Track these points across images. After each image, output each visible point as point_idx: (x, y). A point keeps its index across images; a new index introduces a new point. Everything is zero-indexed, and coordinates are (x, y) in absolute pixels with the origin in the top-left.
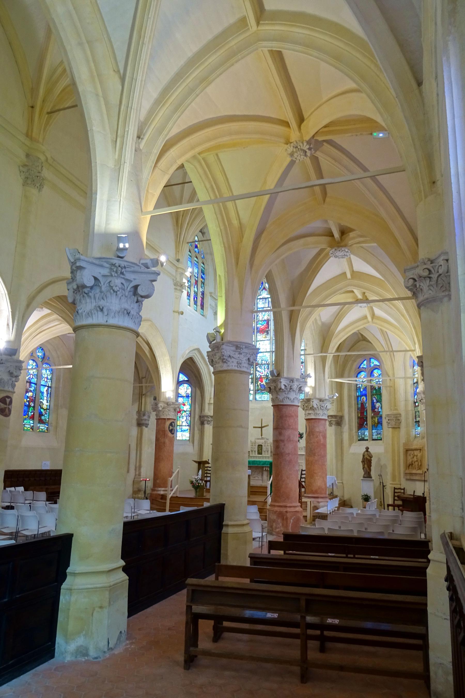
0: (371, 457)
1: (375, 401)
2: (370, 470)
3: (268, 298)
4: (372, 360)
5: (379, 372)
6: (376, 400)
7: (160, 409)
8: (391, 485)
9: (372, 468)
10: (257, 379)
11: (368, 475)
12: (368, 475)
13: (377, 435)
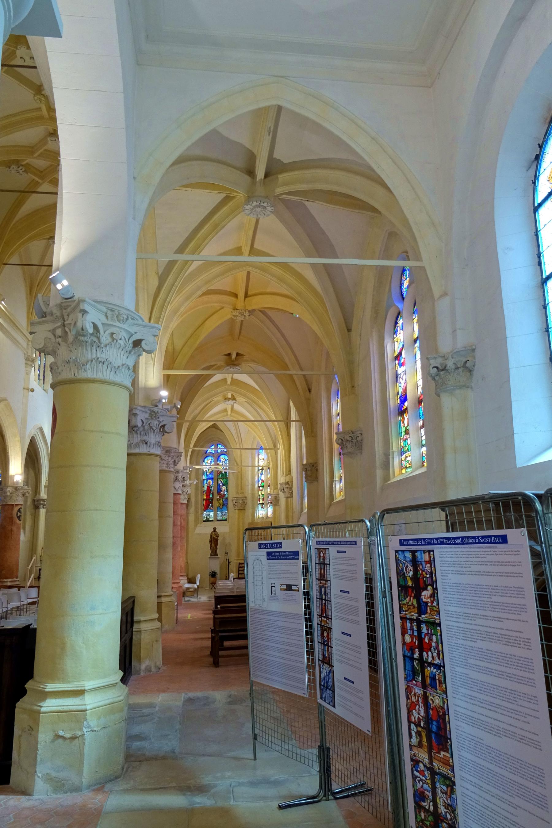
0: (218, 537)
1: (221, 484)
2: (217, 548)
4: (220, 446)
5: (226, 457)
7: (8, 494)
8: (235, 561)
9: (218, 547)
11: (214, 553)
12: (214, 553)
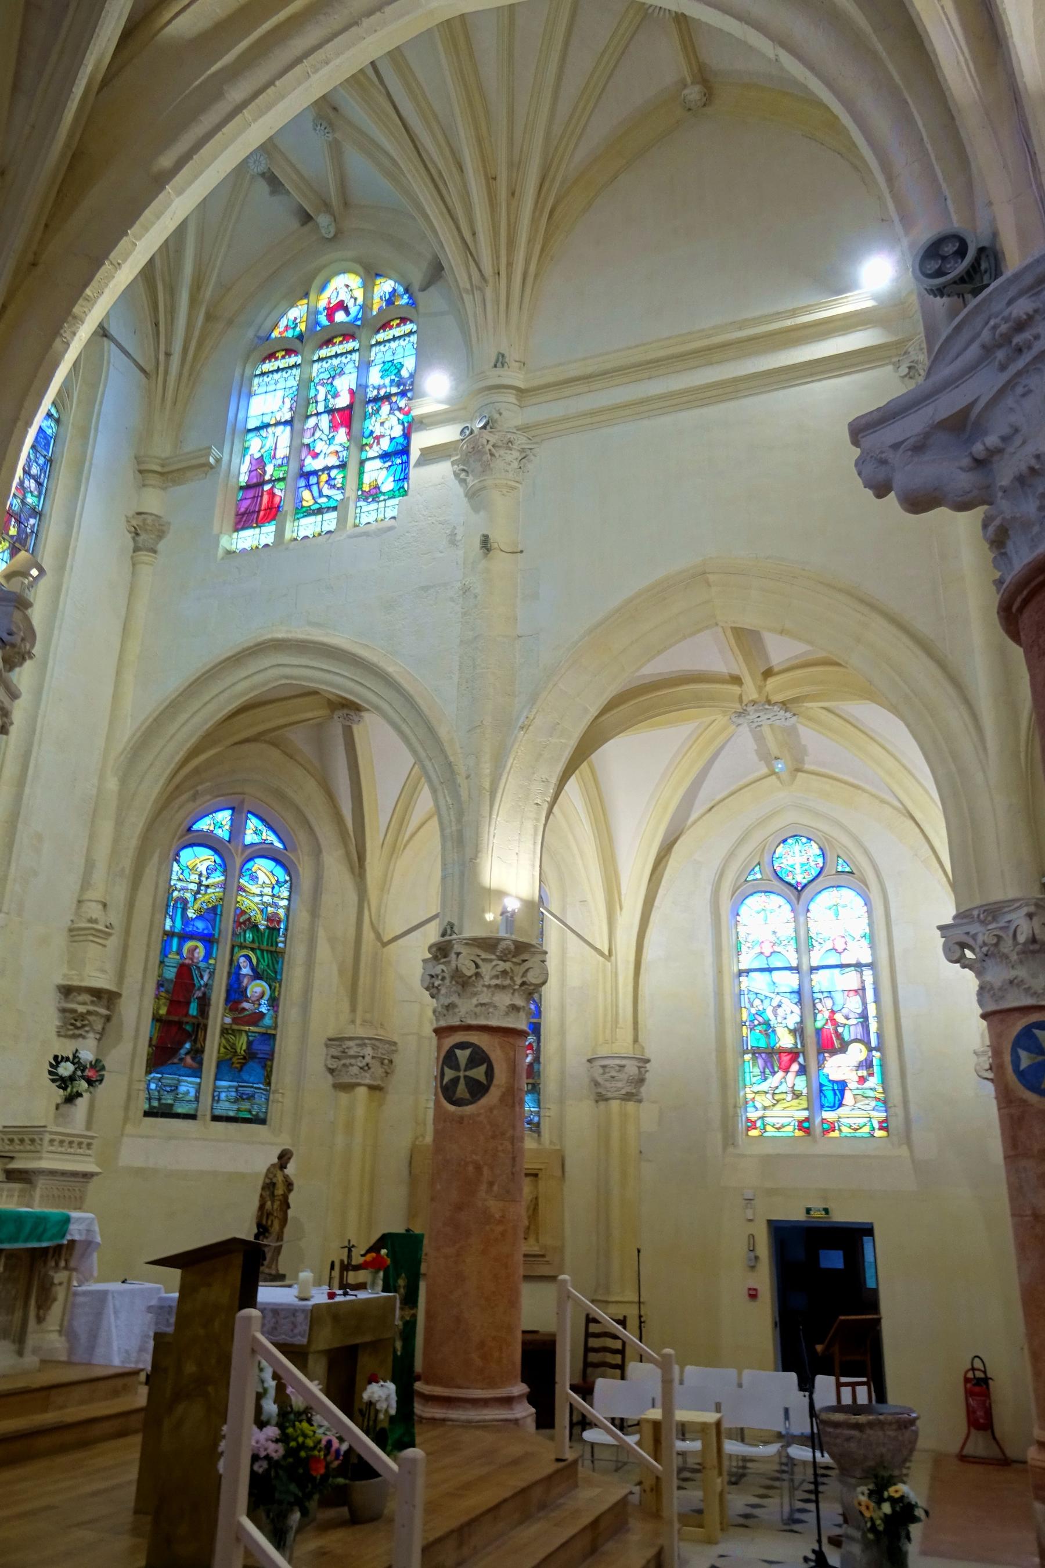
1: (246, 970)
6: (253, 969)
13: (236, 1101)
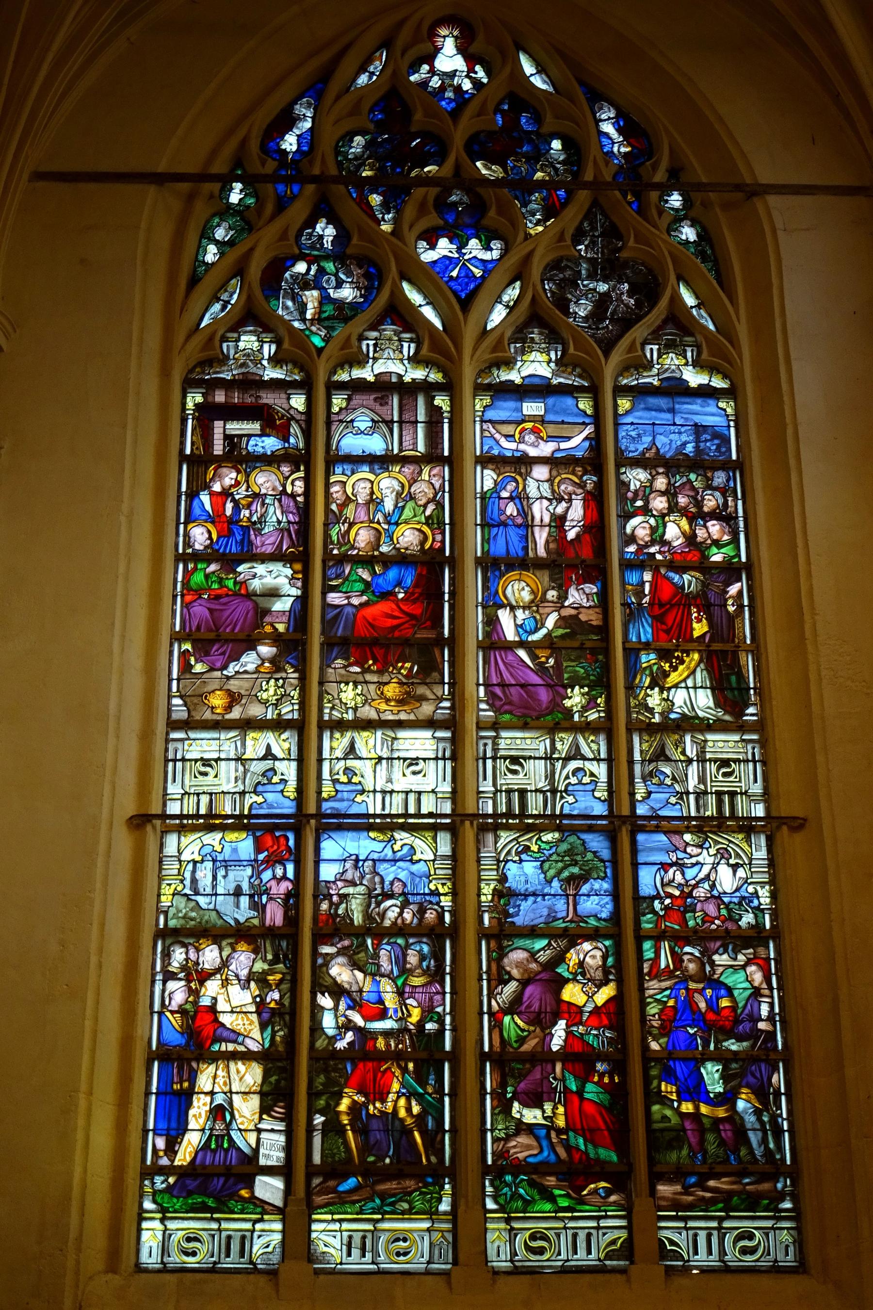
3: (427, 388)
10: (327, 1060)
